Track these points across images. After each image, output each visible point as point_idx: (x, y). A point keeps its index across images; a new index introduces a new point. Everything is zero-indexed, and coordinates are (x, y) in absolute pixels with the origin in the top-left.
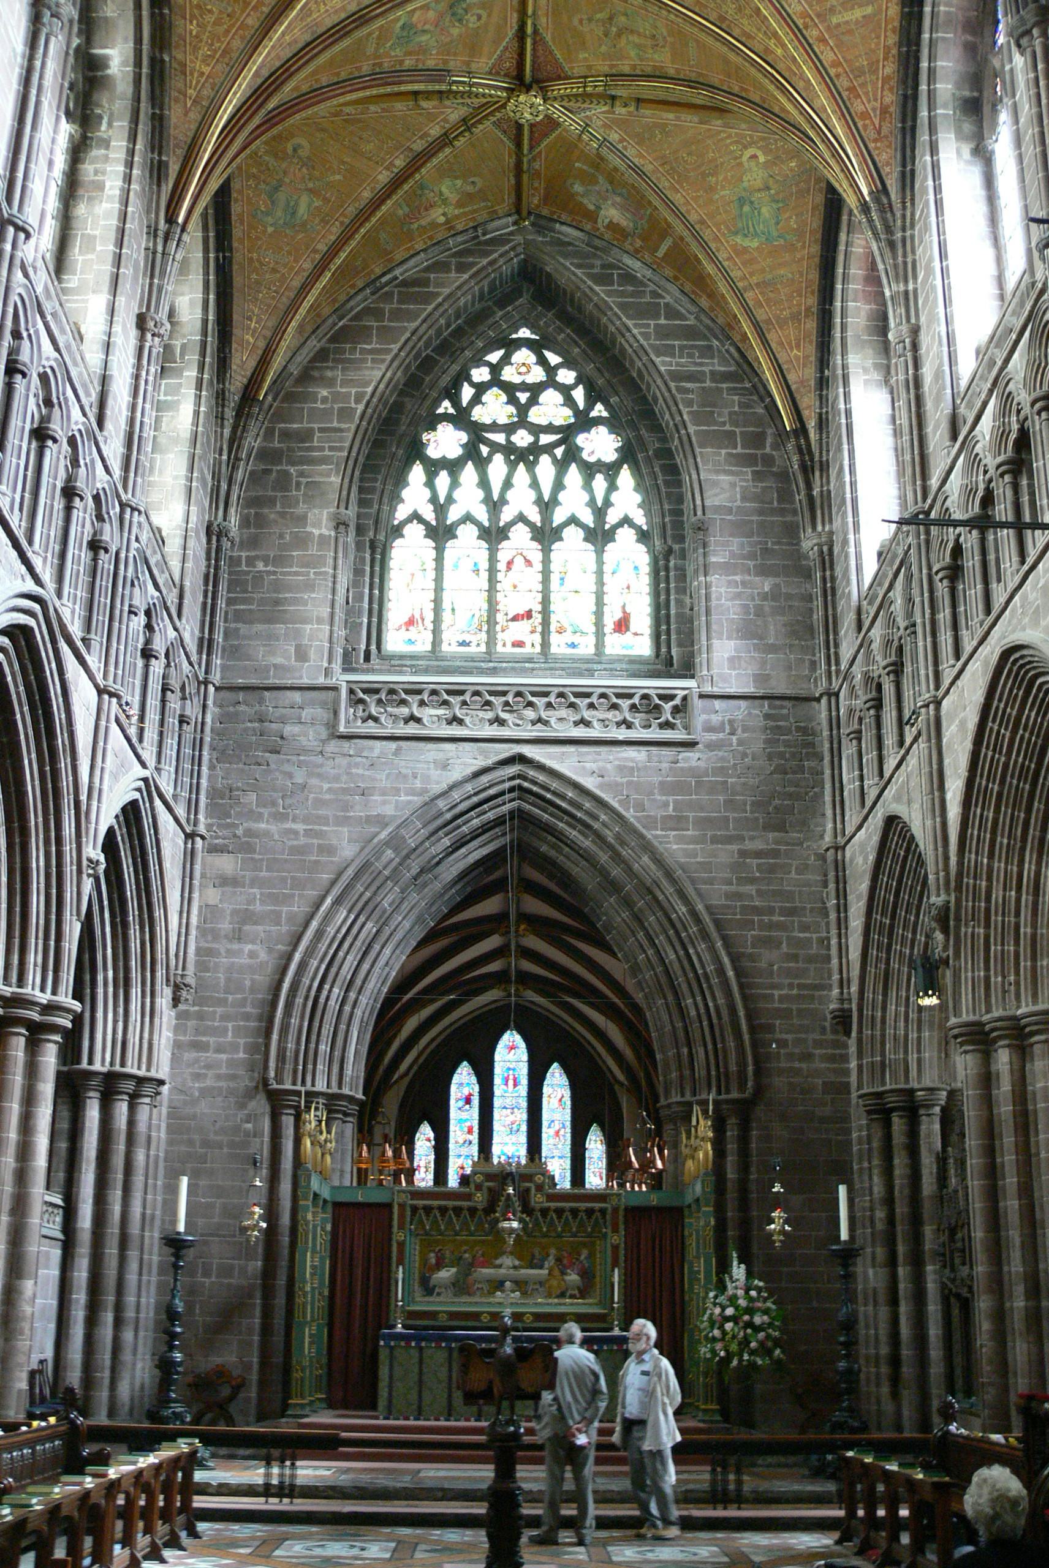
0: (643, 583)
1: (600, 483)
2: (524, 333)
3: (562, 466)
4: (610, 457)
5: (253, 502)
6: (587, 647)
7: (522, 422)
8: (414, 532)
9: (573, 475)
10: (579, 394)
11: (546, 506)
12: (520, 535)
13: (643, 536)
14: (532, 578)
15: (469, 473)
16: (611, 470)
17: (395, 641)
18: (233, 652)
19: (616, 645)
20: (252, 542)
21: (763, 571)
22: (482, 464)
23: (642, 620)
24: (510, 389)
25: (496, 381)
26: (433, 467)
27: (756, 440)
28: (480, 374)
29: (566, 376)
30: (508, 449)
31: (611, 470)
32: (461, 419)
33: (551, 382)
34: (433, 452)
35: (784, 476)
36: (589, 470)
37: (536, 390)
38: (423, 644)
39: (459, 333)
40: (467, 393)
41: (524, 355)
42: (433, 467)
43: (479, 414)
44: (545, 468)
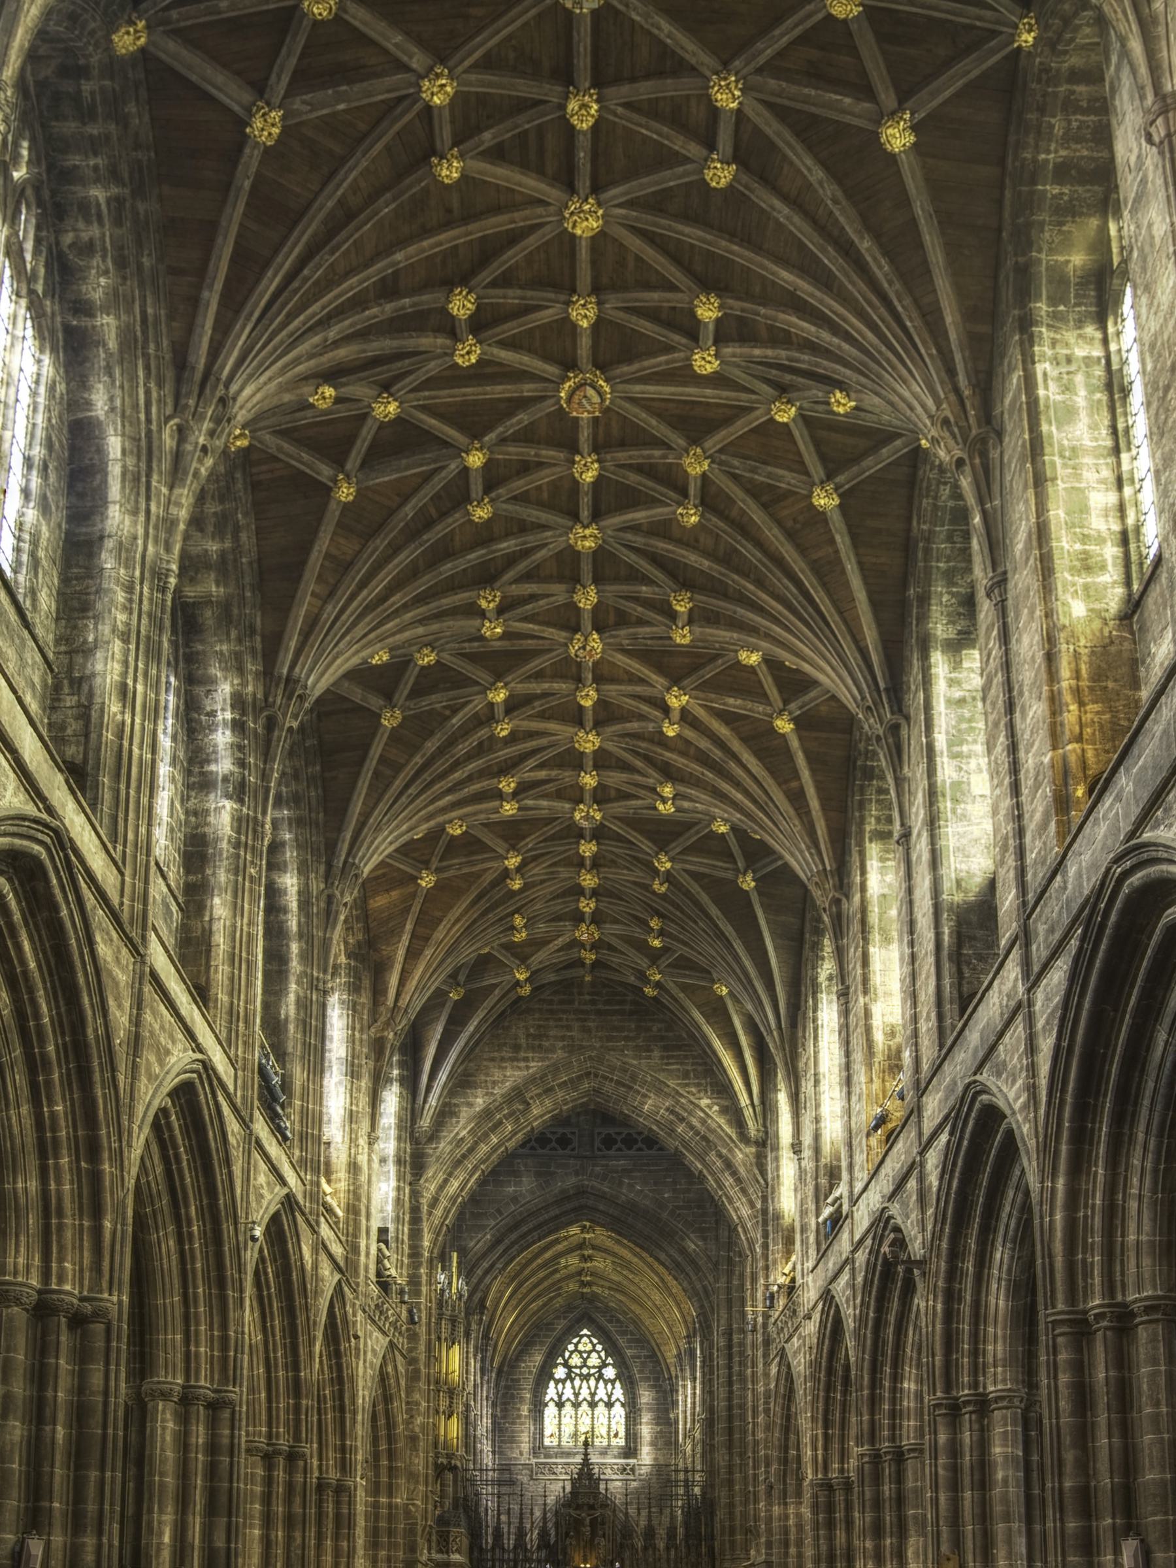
0: (623, 1421)
1: (609, 1386)
2: (585, 1332)
3: (597, 1380)
4: (613, 1377)
5: (504, 1404)
6: (605, 1443)
7: (584, 1365)
8: (552, 1405)
9: (601, 1383)
10: (603, 1354)
11: (593, 1395)
12: (585, 1406)
13: (623, 1405)
14: (588, 1420)
15: (568, 1384)
16: (613, 1382)
17: (547, 1442)
18: (501, 1453)
19: (614, 1442)
20: (504, 1417)
21: (657, 1424)
22: (572, 1380)
23: (622, 1434)
24: (580, 1352)
25: (576, 1350)
26: (557, 1382)
27: (657, 1379)
28: (571, 1347)
29: (599, 1347)
30: (581, 1375)
31: (613, 1382)
32: (566, 1364)
33: (594, 1350)
34: (557, 1376)
35: (665, 1392)
36: (606, 1382)
37: (589, 1352)
38: (555, 1443)
39: (564, 1334)
40: (567, 1354)
41: (585, 1339)
42: (557, 1382)
43: (572, 1362)
44: (592, 1382)
